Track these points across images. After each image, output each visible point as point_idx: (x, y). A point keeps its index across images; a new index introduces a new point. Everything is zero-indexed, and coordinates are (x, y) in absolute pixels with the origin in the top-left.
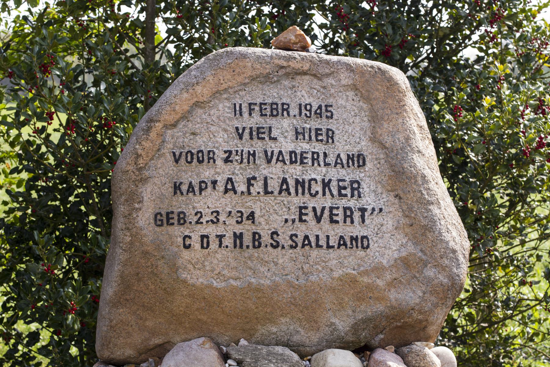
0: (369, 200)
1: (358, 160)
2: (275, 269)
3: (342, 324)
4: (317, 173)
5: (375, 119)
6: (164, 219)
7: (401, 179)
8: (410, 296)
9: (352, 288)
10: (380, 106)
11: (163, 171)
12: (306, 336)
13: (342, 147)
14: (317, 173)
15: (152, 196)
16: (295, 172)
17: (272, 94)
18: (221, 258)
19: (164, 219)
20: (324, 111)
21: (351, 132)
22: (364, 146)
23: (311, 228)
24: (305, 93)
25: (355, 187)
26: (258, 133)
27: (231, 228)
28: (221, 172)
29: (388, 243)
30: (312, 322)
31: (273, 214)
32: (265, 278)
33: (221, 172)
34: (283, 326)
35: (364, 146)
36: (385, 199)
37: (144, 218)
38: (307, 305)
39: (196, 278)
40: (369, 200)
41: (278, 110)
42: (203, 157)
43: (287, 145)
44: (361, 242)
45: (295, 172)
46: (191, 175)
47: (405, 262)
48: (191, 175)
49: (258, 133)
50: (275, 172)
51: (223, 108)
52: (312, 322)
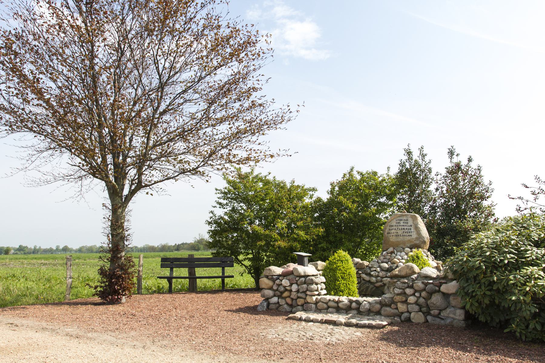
0: (412, 230)
1: (411, 226)
2: (400, 239)
3: (409, 245)
4: (406, 227)
5: (413, 221)
6: (388, 233)
7: (417, 228)
8: (417, 242)
9: (409, 241)
10: (415, 219)
11: (388, 228)
12: (404, 247)
13: (409, 224)
14: (406, 227)
15: (387, 231)
16: (403, 227)
17: (401, 218)
18: (394, 237)
19: (388, 233)
20: (407, 220)
21: (410, 222)
22: (412, 224)
23: (405, 234)
24: (405, 218)
25: (411, 229)
26: (399, 223)
27: (395, 234)
28: (394, 228)
29: (414, 235)
30: (405, 245)
31: (400, 232)
32: (399, 240)
33: (394, 228)
34: (401, 246)
35: (412, 224)
36: (414, 230)
37: (386, 233)
38: (404, 243)
39: (391, 240)
40: (412, 230)
41: (401, 220)
42: (392, 226)
43: (402, 224)
44: (411, 236)
45: (403, 227)
46: (391, 228)
47: (416, 238)
48: (391, 228)
49: (399, 223)
50: (400, 227)
51: (395, 220)
52: (405, 245)
